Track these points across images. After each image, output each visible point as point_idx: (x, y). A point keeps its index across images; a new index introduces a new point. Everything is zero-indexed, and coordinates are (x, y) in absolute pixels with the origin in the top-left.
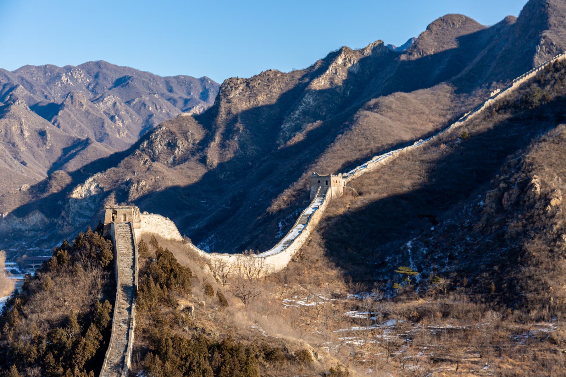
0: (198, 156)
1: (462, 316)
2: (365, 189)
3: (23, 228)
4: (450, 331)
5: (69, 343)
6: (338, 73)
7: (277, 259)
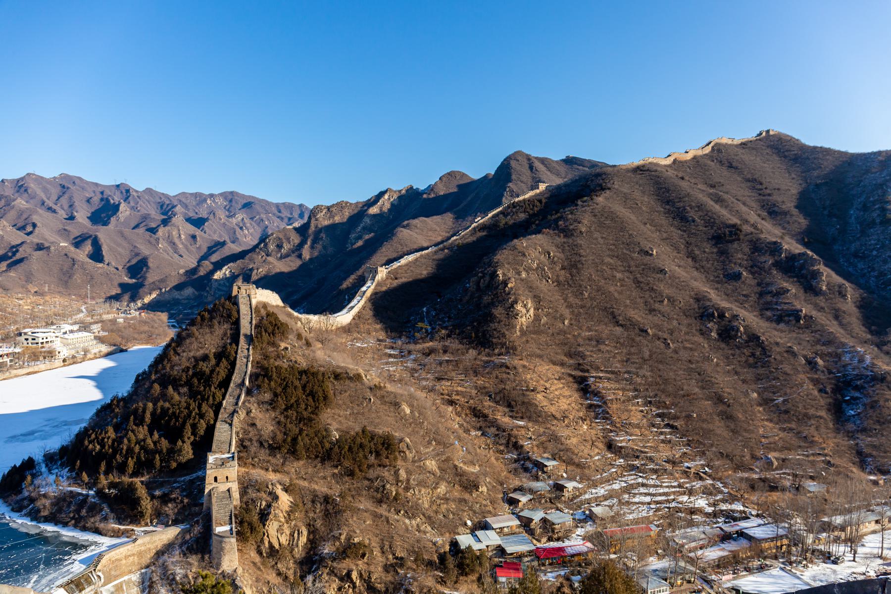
0: (296, 254)
2: (399, 276)
3: (180, 298)
4: (447, 361)
5: (208, 371)
6: (385, 203)
7: (344, 318)
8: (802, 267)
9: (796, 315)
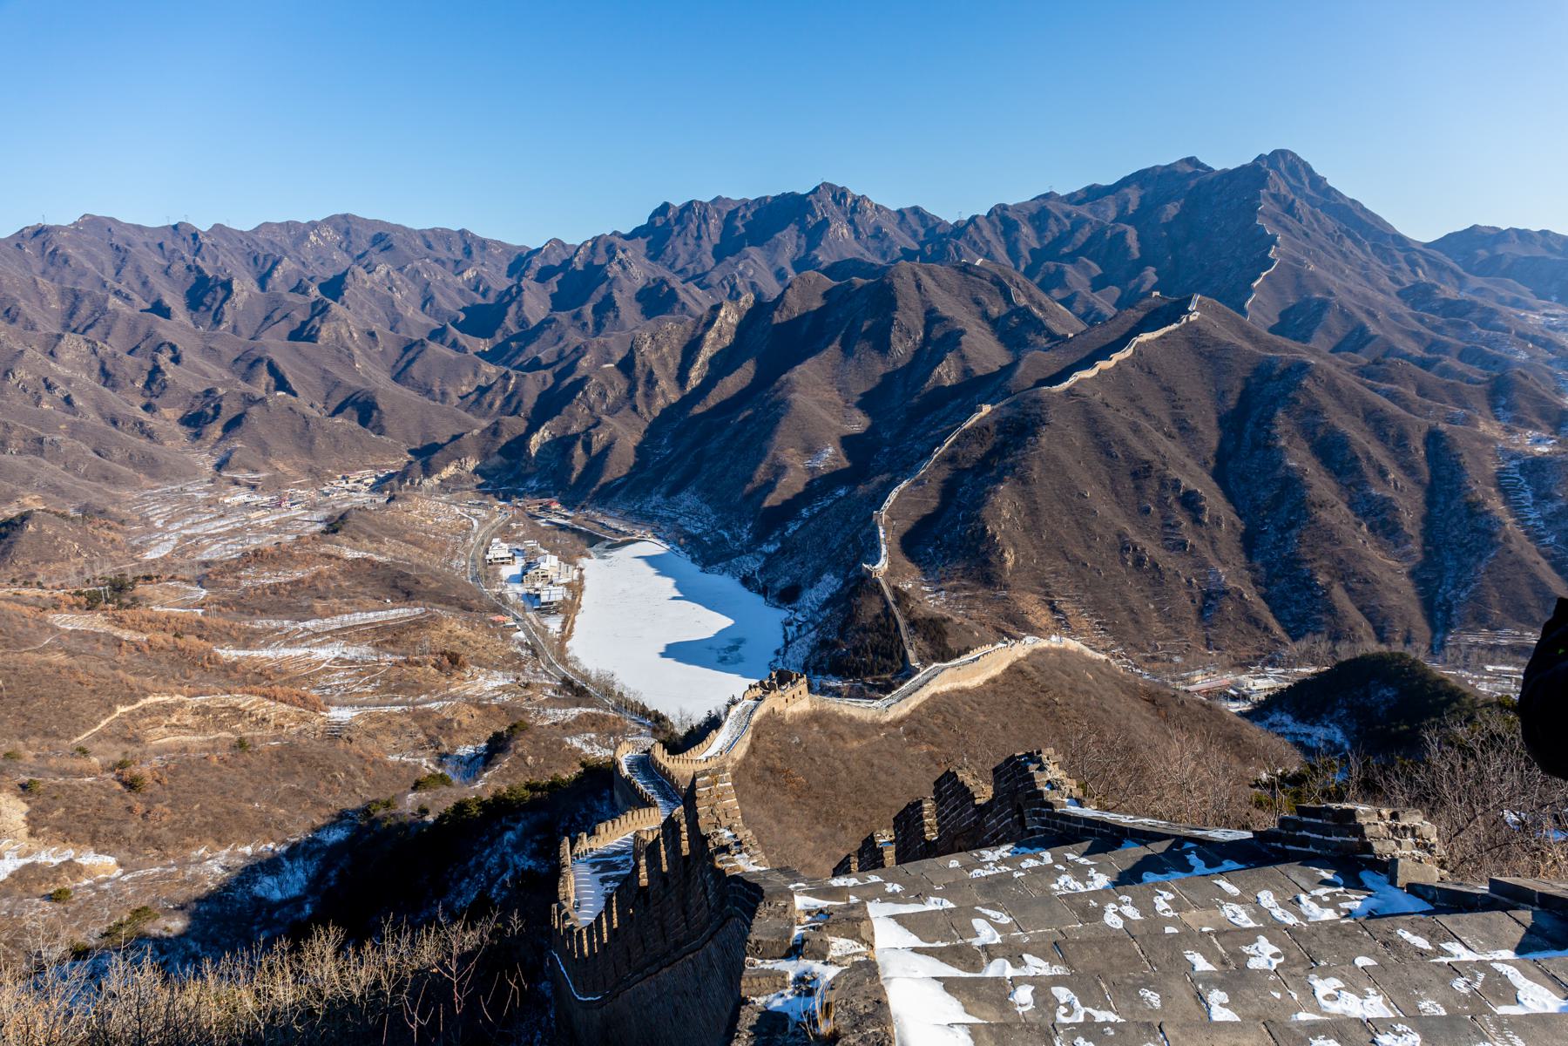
1: (971, 589)
8: (1194, 502)
9: (1183, 544)
